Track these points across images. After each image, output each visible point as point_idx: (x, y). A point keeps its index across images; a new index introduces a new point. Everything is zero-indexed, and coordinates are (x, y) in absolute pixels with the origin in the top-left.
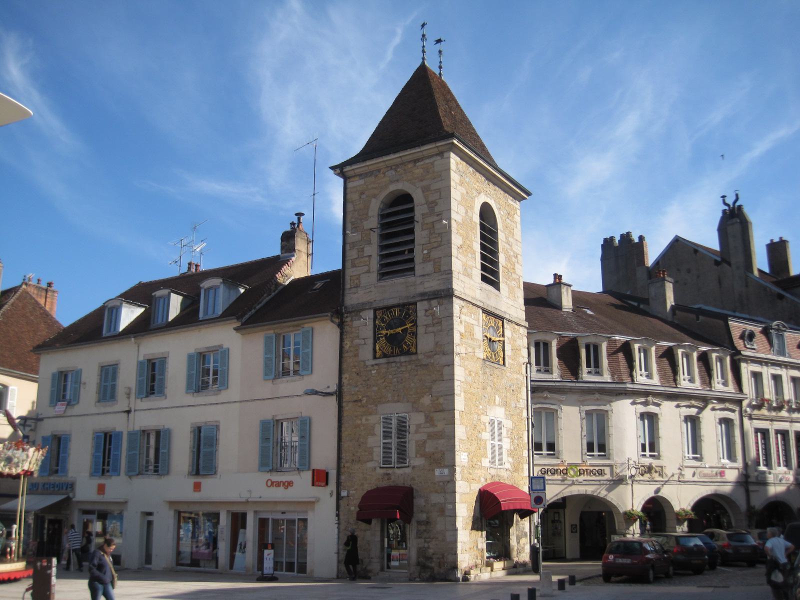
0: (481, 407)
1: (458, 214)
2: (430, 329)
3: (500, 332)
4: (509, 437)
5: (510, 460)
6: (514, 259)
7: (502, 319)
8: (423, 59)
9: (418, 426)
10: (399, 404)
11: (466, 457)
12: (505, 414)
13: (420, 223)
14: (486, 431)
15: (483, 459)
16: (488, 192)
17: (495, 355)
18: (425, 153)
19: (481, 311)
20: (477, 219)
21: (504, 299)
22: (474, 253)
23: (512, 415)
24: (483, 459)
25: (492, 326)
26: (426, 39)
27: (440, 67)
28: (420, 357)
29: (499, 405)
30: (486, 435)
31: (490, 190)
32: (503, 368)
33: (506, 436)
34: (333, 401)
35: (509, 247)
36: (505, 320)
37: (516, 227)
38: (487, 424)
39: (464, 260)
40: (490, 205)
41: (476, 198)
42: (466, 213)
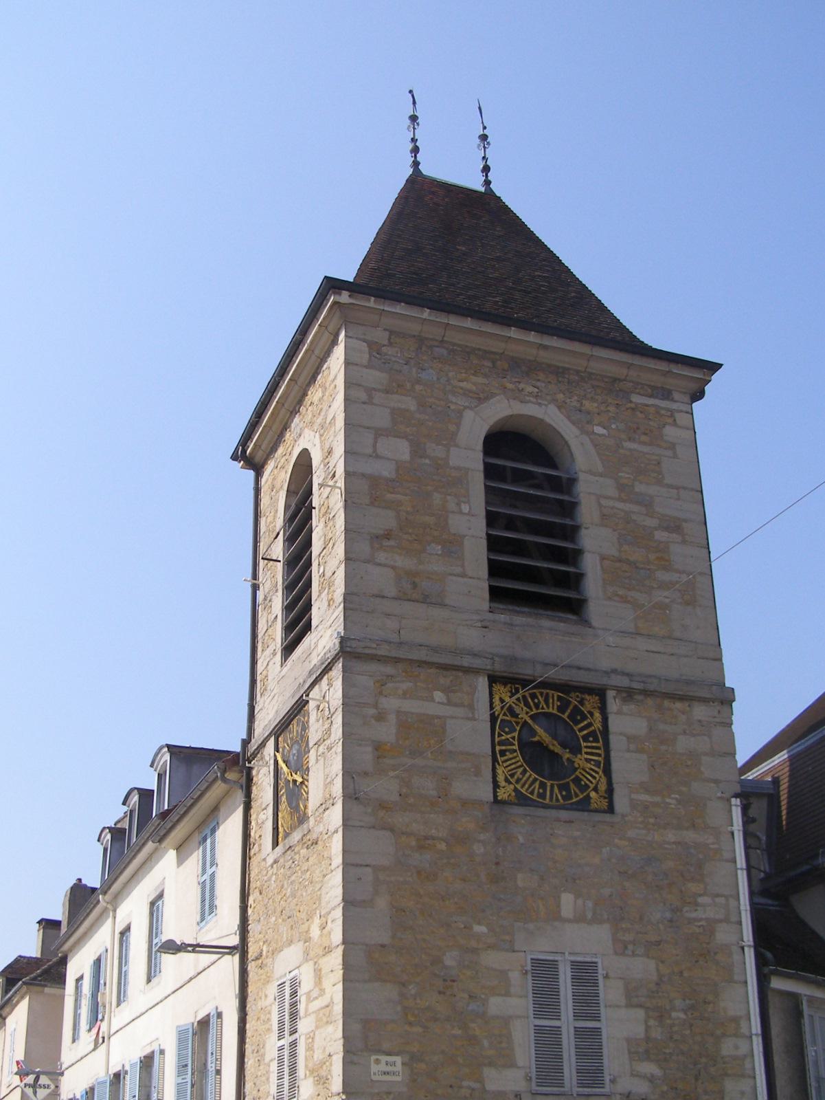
0: (480, 929)
1: (378, 457)
2: (321, 749)
3: (590, 725)
4: (640, 1006)
5: (649, 1068)
6: (661, 535)
7: (600, 693)
8: (416, 164)
9: (308, 994)
10: (293, 946)
11: (399, 1067)
12: (615, 940)
13: (317, 509)
14: (507, 994)
15: (488, 1072)
16: (530, 389)
17: (561, 788)
18: (317, 352)
19: (482, 683)
20: (469, 457)
21: (611, 640)
22: (452, 547)
23: (658, 943)
24: (488, 1072)
25: (548, 716)
26: (418, 124)
27: (486, 169)
28: (312, 821)
29: (580, 919)
30: (515, 1006)
31: (538, 384)
32: (607, 817)
33: (623, 1002)
34: (231, 964)
35: (636, 508)
36: (611, 694)
37: (675, 456)
38: (515, 976)
39: (402, 561)
40: (542, 420)
41: (469, 415)
42: (418, 450)
